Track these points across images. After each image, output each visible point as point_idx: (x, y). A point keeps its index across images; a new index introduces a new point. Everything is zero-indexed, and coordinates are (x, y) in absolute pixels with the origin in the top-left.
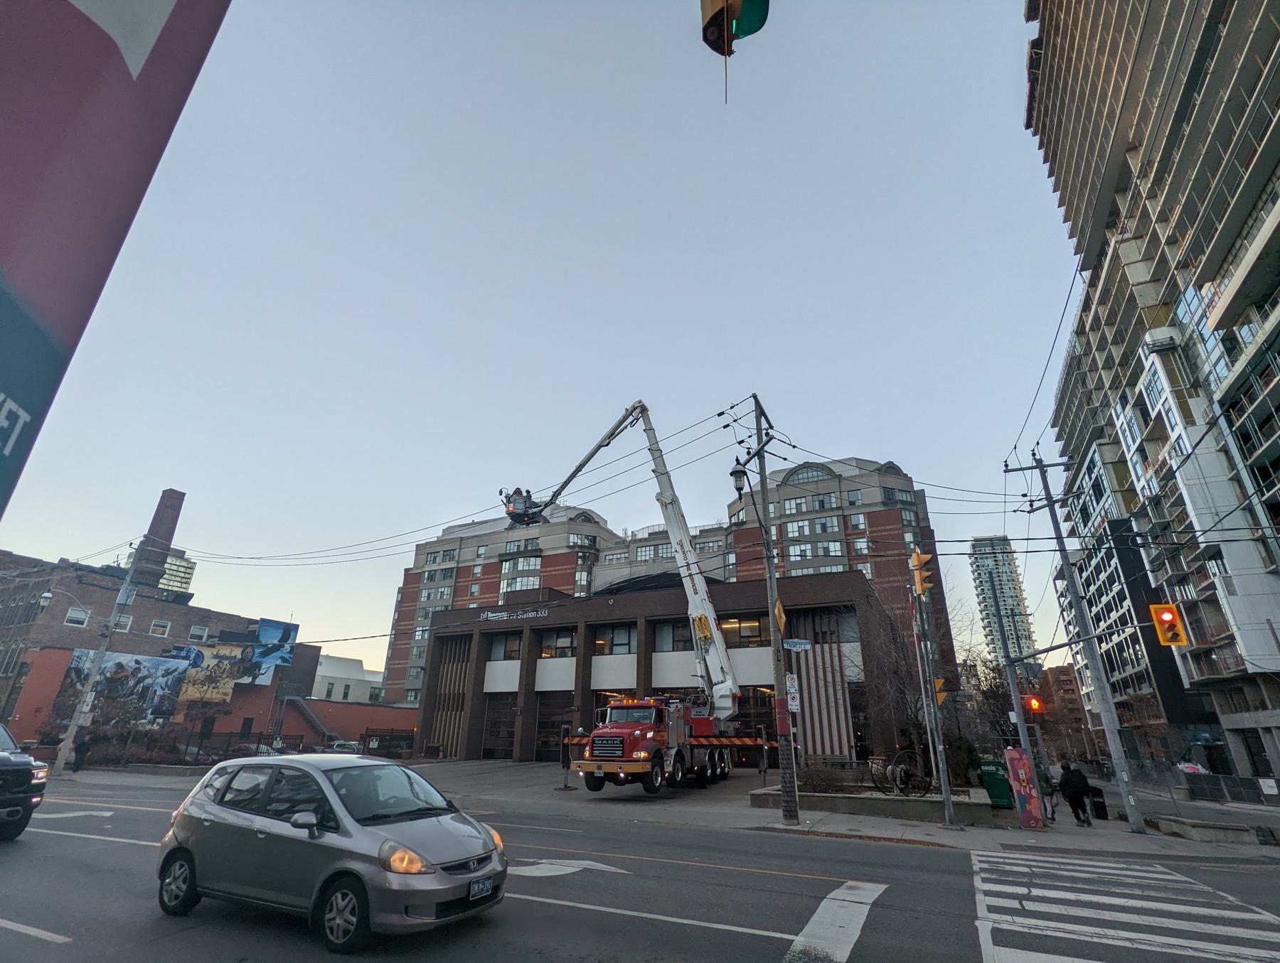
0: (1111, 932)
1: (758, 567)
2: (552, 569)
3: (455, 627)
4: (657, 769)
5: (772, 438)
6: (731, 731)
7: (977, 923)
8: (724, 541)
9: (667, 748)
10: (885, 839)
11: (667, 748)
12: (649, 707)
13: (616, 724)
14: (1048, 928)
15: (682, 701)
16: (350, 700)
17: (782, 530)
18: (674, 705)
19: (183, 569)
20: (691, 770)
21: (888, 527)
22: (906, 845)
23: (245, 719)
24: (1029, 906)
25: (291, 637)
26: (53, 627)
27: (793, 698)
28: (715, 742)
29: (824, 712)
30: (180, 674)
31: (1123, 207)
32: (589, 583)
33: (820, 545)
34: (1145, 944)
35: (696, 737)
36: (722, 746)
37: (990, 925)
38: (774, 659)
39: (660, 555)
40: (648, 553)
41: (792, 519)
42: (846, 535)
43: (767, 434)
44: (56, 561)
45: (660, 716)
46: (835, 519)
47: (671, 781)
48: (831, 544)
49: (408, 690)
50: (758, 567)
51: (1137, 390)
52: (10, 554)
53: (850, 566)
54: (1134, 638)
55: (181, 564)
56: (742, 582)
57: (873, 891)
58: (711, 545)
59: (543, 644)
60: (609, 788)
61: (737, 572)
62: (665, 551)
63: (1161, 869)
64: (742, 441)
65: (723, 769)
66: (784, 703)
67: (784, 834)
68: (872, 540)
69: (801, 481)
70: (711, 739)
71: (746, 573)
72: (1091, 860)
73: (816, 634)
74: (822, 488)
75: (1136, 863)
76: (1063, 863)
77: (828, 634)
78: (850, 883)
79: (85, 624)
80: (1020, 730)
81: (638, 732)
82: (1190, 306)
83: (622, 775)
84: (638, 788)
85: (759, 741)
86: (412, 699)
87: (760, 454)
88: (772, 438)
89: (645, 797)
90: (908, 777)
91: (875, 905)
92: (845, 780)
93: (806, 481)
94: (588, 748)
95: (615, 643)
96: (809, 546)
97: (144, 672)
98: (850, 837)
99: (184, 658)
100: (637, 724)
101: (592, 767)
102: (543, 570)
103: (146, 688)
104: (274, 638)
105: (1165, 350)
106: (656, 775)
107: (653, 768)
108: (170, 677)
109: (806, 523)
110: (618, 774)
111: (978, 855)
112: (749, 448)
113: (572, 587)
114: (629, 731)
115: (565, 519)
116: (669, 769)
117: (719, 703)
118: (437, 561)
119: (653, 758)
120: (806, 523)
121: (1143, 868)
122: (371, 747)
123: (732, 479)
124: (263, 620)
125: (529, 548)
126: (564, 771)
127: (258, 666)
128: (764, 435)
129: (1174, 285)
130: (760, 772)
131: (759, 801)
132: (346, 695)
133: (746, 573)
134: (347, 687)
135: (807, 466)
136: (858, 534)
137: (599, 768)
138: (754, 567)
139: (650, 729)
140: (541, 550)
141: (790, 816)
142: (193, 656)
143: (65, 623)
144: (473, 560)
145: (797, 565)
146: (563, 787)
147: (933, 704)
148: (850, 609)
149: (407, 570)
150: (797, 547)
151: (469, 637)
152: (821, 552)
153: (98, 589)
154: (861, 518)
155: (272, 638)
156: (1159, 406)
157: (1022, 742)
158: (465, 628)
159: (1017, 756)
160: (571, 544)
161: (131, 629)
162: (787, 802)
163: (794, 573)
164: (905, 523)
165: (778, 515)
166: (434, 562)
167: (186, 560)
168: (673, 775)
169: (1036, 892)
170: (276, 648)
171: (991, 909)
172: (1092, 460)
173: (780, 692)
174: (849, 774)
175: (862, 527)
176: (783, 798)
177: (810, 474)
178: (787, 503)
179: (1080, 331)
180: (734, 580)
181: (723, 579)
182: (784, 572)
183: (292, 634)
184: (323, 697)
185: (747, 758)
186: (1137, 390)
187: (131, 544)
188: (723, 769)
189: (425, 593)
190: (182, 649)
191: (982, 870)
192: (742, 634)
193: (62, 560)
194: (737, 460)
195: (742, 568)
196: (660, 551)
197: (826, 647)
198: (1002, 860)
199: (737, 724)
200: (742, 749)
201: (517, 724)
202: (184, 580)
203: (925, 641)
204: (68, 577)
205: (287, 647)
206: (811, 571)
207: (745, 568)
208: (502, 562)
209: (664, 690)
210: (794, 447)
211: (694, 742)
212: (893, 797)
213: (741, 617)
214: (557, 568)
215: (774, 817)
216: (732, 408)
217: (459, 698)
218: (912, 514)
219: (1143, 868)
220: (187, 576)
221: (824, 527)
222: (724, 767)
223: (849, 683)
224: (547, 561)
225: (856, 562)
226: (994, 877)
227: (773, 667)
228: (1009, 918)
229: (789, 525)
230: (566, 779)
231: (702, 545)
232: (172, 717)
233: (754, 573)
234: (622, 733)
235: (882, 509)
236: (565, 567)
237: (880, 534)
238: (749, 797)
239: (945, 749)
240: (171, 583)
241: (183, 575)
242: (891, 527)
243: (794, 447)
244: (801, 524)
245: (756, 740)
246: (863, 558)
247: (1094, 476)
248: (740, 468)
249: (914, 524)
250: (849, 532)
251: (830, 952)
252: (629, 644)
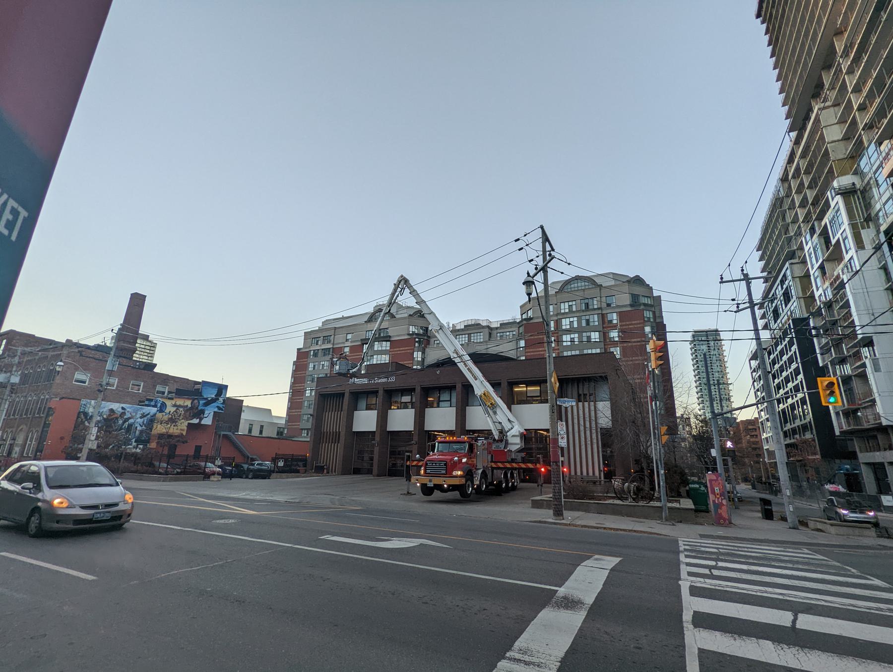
0: (770, 589)
1: (541, 349)
2: (398, 349)
3: (333, 388)
4: (469, 482)
5: (554, 257)
6: (519, 459)
7: (680, 582)
8: (517, 331)
9: (476, 469)
10: (621, 530)
11: (476, 469)
12: (464, 442)
13: (441, 453)
14: (727, 586)
15: (486, 438)
16: (264, 435)
17: (558, 323)
18: (481, 441)
19: (148, 348)
20: (491, 484)
21: (633, 322)
22: (635, 534)
23: (196, 446)
24: (716, 572)
25: (223, 393)
27: (562, 438)
28: (508, 465)
29: (583, 447)
30: (152, 416)
31: (827, 81)
32: (423, 359)
33: (584, 334)
34: (792, 597)
35: (494, 462)
36: (513, 469)
37: (688, 584)
38: (550, 412)
39: (472, 341)
40: (463, 339)
41: (565, 316)
42: (603, 328)
43: (550, 255)
44: (64, 342)
45: (471, 448)
46: (596, 316)
47: (478, 490)
48: (593, 334)
49: (302, 429)
50: (541, 349)
51: (823, 223)
52: (33, 336)
53: (605, 349)
54: (803, 401)
55: (147, 344)
56: (530, 359)
57: (612, 562)
58: (508, 334)
59: (392, 400)
60: (437, 494)
61: (526, 353)
62: (475, 338)
63: (806, 551)
64: (532, 260)
65: (513, 484)
66: (556, 441)
67: (553, 526)
68: (622, 331)
69: (573, 289)
70: (506, 464)
71: (532, 354)
72: (759, 545)
73: (579, 395)
74: (588, 294)
75: (789, 548)
76: (740, 547)
77: (588, 395)
78: (597, 556)
79: (87, 383)
80: (717, 461)
81: (456, 458)
82: (870, 160)
83: (445, 486)
84: (456, 494)
85: (538, 466)
86: (305, 435)
87: (544, 269)
88: (554, 257)
89: (462, 500)
90: (638, 490)
91: (612, 570)
92: (597, 492)
93: (577, 289)
94: (423, 468)
95: (441, 400)
96: (576, 335)
97: (128, 415)
98: (598, 528)
99: (154, 406)
100: (455, 453)
101: (426, 480)
102: (391, 350)
103: (130, 426)
104: (212, 394)
105: (847, 193)
106: (469, 486)
107: (466, 482)
108: (145, 418)
109: (575, 319)
110: (443, 485)
111: (684, 541)
112: (536, 265)
113: (412, 362)
114: (450, 457)
115: (406, 315)
116: (477, 482)
117: (511, 440)
118: (319, 344)
119: (466, 475)
120: (575, 319)
121: (795, 551)
122: (279, 465)
123: (524, 287)
124: (203, 382)
125: (382, 335)
126: (407, 482)
127: (203, 412)
128: (548, 255)
129: (860, 143)
130: (538, 486)
131: (537, 505)
132: (261, 432)
133: (532, 354)
134: (262, 427)
135: (578, 278)
136: (612, 327)
137: (430, 481)
138: (538, 349)
139: (465, 456)
140: (390, 337)
141: (558, 514)
142: (159, 405)
143: (74, 383)
144: (344, 343)
145: (568, 348)
146: (406, 492)
147: (659, 442)
148: (604, 378)
149: (299, 350)
150: (568, 336)
151: (342, 395)
152: (585, 339)
153: (94, 360)
154: (615, 316)
155: (211, 394)
156: (838, 235)
157: (719, 469)
158: (339, 389)
159: (715, 478)
160: (411, 332)
161: (117, 385)
162: (556, 505)
163: (565, 354)
164: (646, 319)
165: (556, 313)
166: (317, 344)
167: (150, 341)
168: (479, 486)
169: (720, 564)
170: (214, 401)
171: (690, 574)
172: (785, 275)
173: (553, 433)
174: (599, 488)
175: (615, 322)
176: (553, 503)
177: (579, 284)
178: (562, 305)
179: (784, 179)
180: (524, 358)
181: (515, 358)
182: (559, 353)
183: (224, 391)
184: (246, 433)
185: (530, 476)
186: (823, 223)
187: (113, 330)
188: (513, 484)
189: (311, 365)
190: (151, 400)
191: (685, 550)
192: (528, 395)
193: (68, 341)
194: (528, 273)
195: (529, 350)
196: (472, 338)
197: (586, 404)
198: (699, 544)
199: (523, 454)
200: (526, 471)
201: (375, 453)
202: (149, 355)
203: (656, 401)
204: (73, 351)
205: (221, 400)
206: (577, 352)
207: (531, 350)
208: (363, 344)
209: (474, 431)
210: (569, 264)
211: (494, 466)
212: (628, 503)
213: (528, 383)
214: (401, 349)
215: (547, 515)
216: (525, 235)
217: (336, 436)
218: (651, 313)
219: (795, 551)
220: (151, 352)
221: (588, 322)
222: (514, 482)
223: (601, 429)
224: (394, 344)
225: (609, 346)
226: (693, 554)
227: (548, 417)
228: (702, 580)
229: (563, 320)
230: (408, 488)
231: (501, 334)
232: (148, 444)
233: (538, 353)
234: (447, 459)
235: (629, 309)
236: (407, 348)
237: (627, 327)
238: (531, 501)
239: (665, 473)
240: (141, 357)
241: (148, 351)
242: (636, 322)
243: (569, 264)
244: (571, 319)
245: (536, 465)
246: (614, 344)
247: (785, 287)
248: (530, 279)
249: (652, 320)
250: (604, 326)
251: (582, 597)
252: (450, 401)
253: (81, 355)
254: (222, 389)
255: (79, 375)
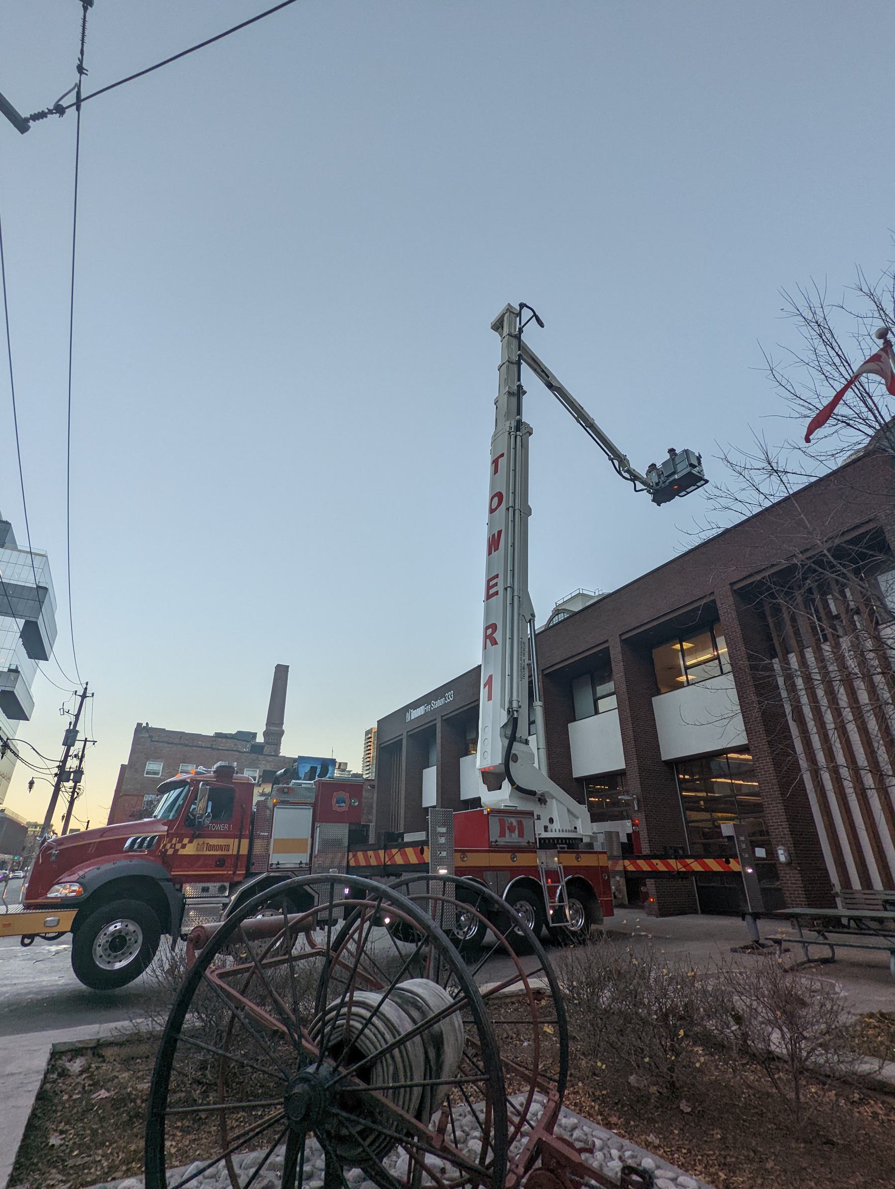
25: (330, 772)
26: (136, 779)
124: (301, 758)
143: (145, 775)
153: (166, 745)
187: (76, 691)
193: (239, 732)
253: (152, 741)
254: (327, 764)
255: (151, 765)
